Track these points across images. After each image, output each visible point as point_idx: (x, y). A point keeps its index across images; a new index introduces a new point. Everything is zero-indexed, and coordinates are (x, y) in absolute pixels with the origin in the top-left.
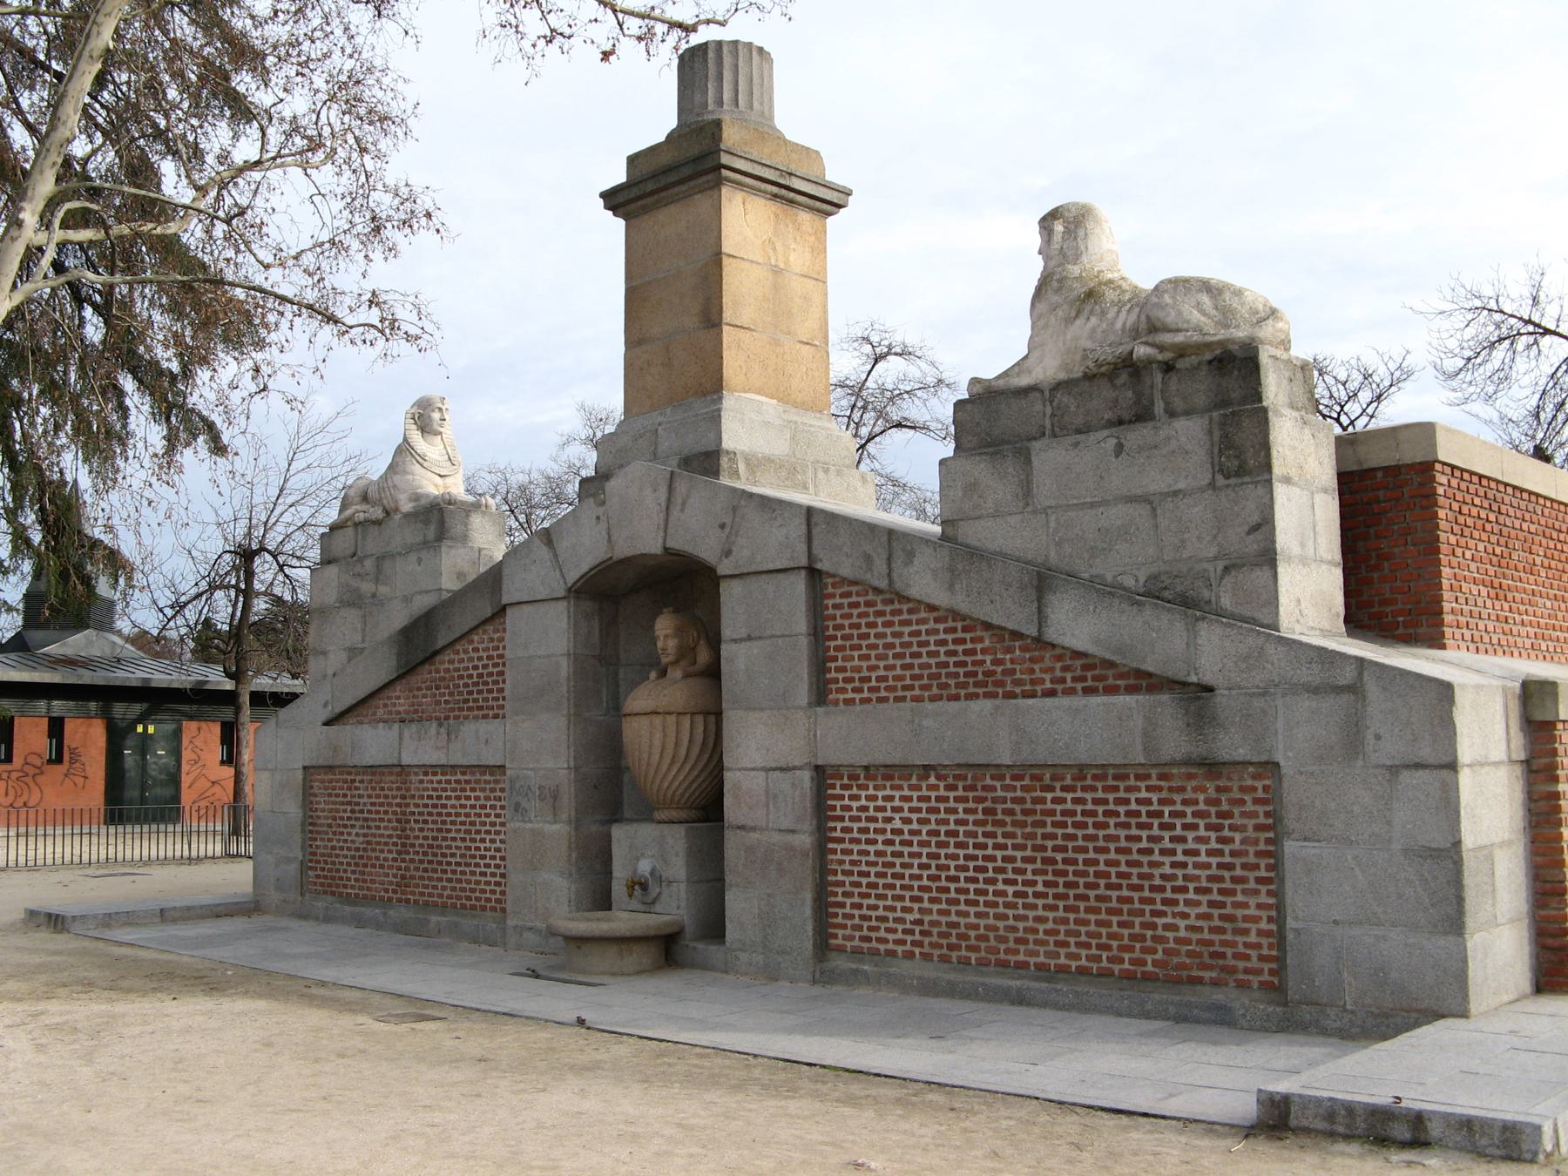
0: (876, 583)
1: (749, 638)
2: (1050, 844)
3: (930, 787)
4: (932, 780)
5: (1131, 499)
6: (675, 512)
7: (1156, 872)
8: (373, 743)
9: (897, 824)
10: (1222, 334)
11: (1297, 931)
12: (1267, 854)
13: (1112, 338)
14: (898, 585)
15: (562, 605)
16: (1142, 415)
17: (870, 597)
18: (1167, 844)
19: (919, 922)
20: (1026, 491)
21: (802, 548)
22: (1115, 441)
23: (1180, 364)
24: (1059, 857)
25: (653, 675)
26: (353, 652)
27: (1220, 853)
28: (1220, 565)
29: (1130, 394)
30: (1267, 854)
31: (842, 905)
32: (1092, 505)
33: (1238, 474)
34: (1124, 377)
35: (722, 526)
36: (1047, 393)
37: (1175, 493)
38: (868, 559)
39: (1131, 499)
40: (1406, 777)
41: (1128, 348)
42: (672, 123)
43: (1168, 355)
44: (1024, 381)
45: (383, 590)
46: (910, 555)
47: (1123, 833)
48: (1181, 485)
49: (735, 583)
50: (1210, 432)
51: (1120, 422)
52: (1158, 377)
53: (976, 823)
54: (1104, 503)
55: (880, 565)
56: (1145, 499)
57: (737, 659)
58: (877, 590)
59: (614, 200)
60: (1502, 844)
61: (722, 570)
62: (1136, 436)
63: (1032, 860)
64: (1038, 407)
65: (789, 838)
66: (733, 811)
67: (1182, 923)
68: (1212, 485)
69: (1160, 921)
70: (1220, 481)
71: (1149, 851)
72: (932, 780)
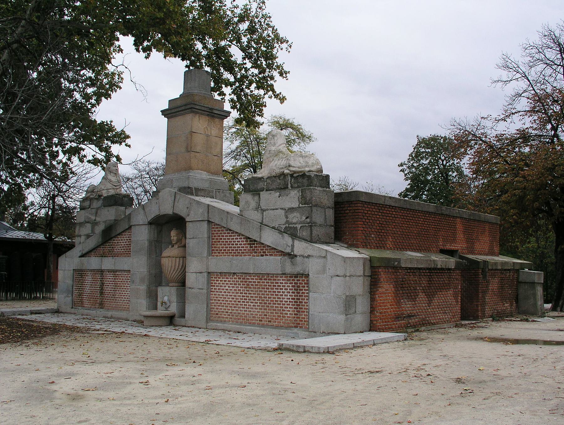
1: (193, 238)
2: (261, 293)
3: (235, 278)
4: (235, 277)
6: (176, 203)
7: (284, 300)
8: (94, 262)
9: (227, 288)
11: (312, 315)
12: (307, 296)
15: (147, 226)
18: (286, 294)
19: (232, 313)
21: (206, 214)
24: (263, 296)
25: (170, 246)
26: (88, 236)
27: (297, 296)
30: (307, 296)
31: (214, 308)
35: (188, 208)
38: (222, 219)
40: (335, 278)
42: (181, 91)
45: (98, 219)
47: (277, 291)
49: (190, 223)
51: (281, 189)
53: (245, 287)
55: (225, 221)
57: (191, 243)
59: (164, 113)
60: (359, 295)
61: (187, 219)
62: (283, 192)
63: (257, 297)
65: (201, 291)
66: (188, 283)
67: (289, 313)
69: (284, 312)
71: (282, 295)
72: (235, 277)
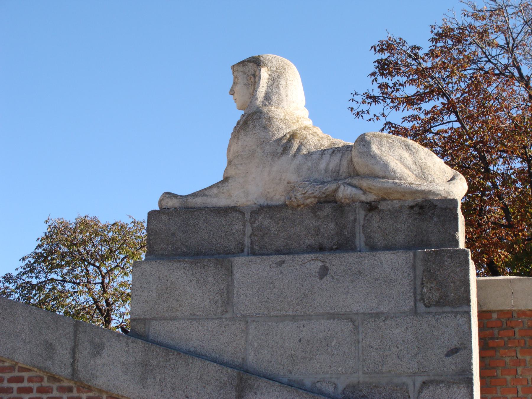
0: (56, 370)
5: (333, 316)
10: (425, 186)
13: (316, 176)
14: (82, 374)
16: (344, 245)
17: (45, 383)
20: (227, 299)
22: (320, 264)
23: (382, 206)
28: (419, 380)
29: (332, 225)
32: (294, 318)
33: (438, 304)
34: (327, 210)
36: (248, 216)
37: (378, 315)
38: (49, 347)
39: (333, 316)
41: (331, 187)
43: (371, 198)
44: (222, 202)
46: (98, 349)
48: (384, 308)
50: (414, 267)
51: (321, 249)
52: (361, 214)
54: (308, 317)
55: (63, 354)
56: (348, 317)
58: (53, 378)
62: (337, 261)
64: (239, 226)
68: (415, 312)
70: (421, 307)
